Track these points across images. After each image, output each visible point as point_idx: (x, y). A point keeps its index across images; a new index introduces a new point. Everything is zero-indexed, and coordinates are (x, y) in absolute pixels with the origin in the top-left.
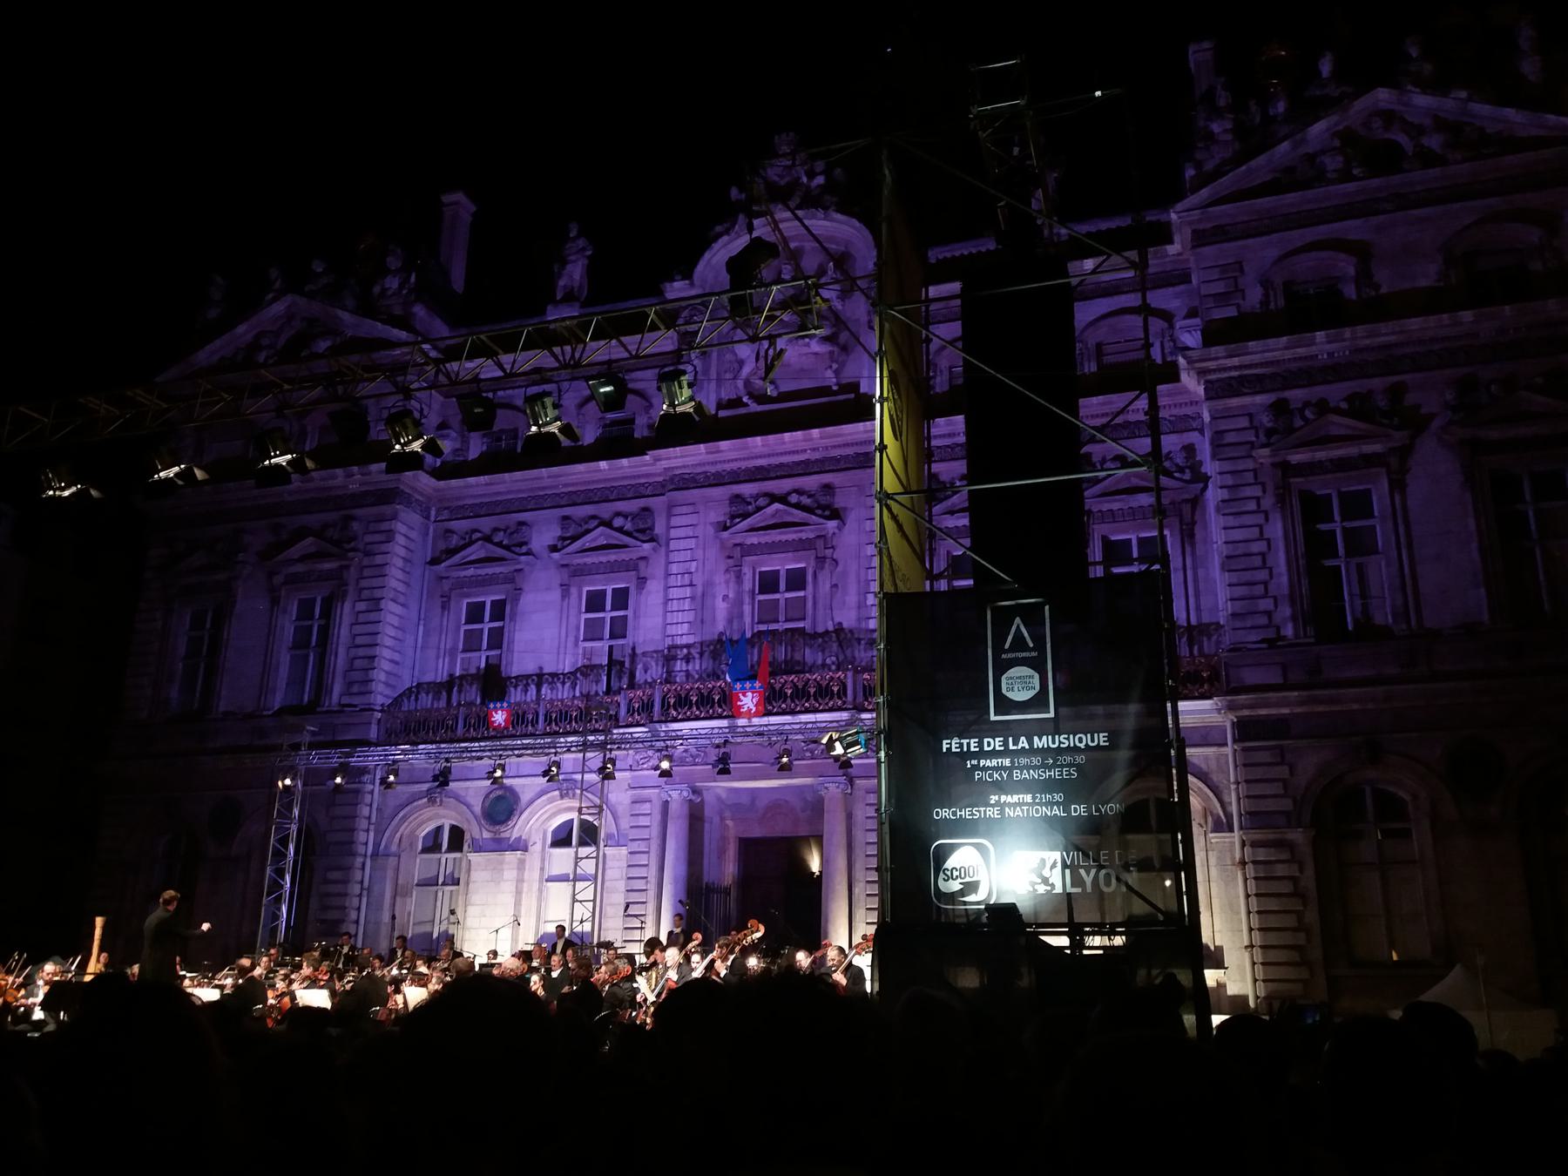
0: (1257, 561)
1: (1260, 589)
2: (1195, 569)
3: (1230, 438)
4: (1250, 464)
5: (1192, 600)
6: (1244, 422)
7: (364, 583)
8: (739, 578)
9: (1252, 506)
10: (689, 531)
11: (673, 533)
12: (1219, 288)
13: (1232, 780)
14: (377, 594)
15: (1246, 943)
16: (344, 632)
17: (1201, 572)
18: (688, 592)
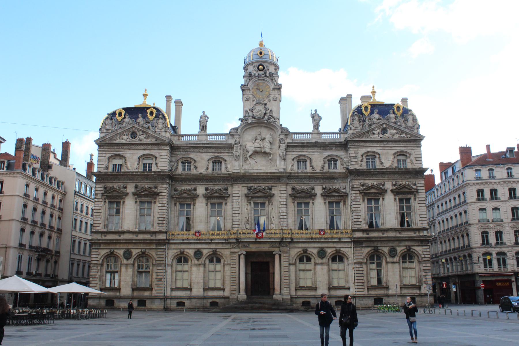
0: (359, 211)
1: (359, 217)
2: (346, 210)
3: (355, 186)
4: (358, 192)
5: (345, 216)
6: (358, 184)
7: (160, 200)
8: (250, 203)
9: (358, 200)
10: (238, 192)
11: (234, 192)
12: (354, 155)
13: (353, 253)
14: (164, 202)
15: (354, 282)
17: (347, 211)
18: (238, 206)
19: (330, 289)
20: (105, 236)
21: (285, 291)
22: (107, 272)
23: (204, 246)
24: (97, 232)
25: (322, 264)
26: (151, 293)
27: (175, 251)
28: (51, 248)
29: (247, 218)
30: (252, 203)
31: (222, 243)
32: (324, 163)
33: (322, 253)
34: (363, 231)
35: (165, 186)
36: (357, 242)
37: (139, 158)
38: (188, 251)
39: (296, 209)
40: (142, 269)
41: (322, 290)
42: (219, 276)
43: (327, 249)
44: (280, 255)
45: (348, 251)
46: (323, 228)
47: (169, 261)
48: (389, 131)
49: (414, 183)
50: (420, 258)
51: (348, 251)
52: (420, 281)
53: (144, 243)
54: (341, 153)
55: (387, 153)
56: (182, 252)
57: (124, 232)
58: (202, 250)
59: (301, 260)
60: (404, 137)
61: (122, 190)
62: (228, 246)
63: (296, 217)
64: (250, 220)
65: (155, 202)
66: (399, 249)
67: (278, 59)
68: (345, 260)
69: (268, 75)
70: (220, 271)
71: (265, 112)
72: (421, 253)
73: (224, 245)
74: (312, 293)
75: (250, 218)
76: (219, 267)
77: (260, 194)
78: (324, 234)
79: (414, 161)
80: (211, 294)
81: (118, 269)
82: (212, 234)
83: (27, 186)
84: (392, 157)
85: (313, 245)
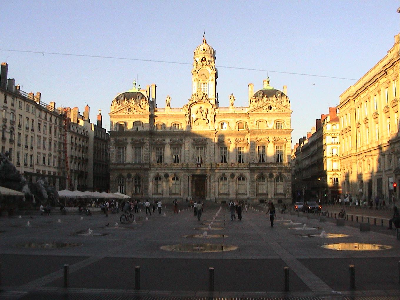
8: (195, 148)
12: (252, 121)
16: (143, 153)
19: (236, 194)
20: (117, 166)
21: (212, 196)
22: (118, 185)
23: (170, 171)
24: (112, 164)
25: (232, 181)
26: (142, 196)
27: (154, 174)
28: (83, 171)
29: (193, 156)
30: (196, 148)
31: (179, 170)
32: (236, 125)
33: (232, 176)
34: (255, 164)
35: (148, 139)
36: (252, 170)
37: (133, 123)
38: (161, 174)
39: (220, 151)
40: (137, 183)
41: (232, 196)
42: (177, 187)
43: (235, 174)
44: (210, 177)
45: (247, 174)
46: (234, 162)
47: (151, 179)
48: (272, 108)
49: (285, 138)
50: (286, 180)
51: (247, 174)
52: (285, 191)
53: (137, 170)
54: (245, 119)
55: (271, 120)
56: (158, 174)
57: (127, 164)
58: (168, 174)
59: (222, 179)
60: (281, 111)
61: (125, 141)
62: (183, 171)
63: (220, 156)
64: (194, 157)
65: (143, 148)
66: (274, 174)
67: (215, 52)
68: (245, 179)
69: (208, 64)
70: (178, 184)
71: (203, 96)
72: (287, 176)
73: (181, 171)
74: (227, 197)
75: (194, 156)
76: (178, 182)
77: (200, 143)
78: (234, 165)
79: (286, 125)
80: (173, 197)
81: (124, 184)
82: (174, 165)
83: (72, 137)
84: (273, 122)
85: (228, 171)
